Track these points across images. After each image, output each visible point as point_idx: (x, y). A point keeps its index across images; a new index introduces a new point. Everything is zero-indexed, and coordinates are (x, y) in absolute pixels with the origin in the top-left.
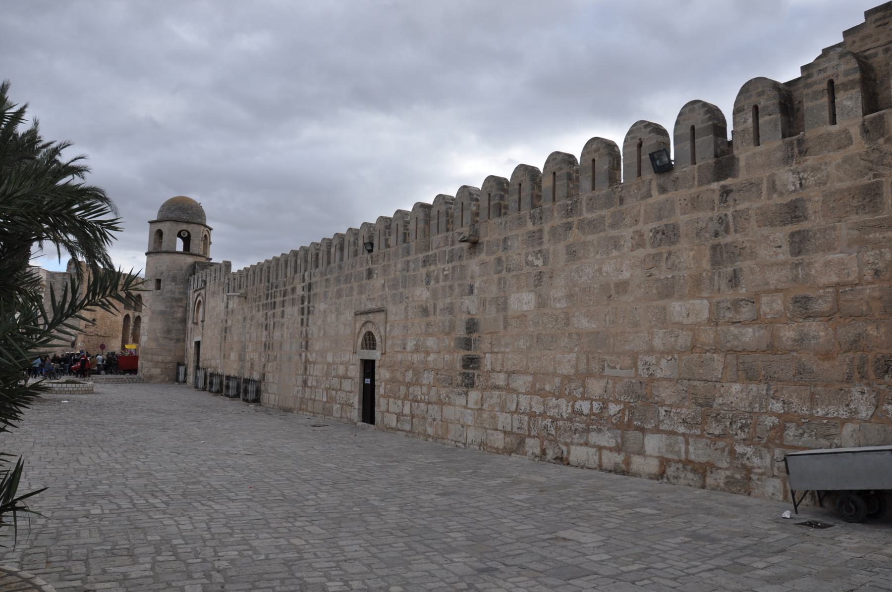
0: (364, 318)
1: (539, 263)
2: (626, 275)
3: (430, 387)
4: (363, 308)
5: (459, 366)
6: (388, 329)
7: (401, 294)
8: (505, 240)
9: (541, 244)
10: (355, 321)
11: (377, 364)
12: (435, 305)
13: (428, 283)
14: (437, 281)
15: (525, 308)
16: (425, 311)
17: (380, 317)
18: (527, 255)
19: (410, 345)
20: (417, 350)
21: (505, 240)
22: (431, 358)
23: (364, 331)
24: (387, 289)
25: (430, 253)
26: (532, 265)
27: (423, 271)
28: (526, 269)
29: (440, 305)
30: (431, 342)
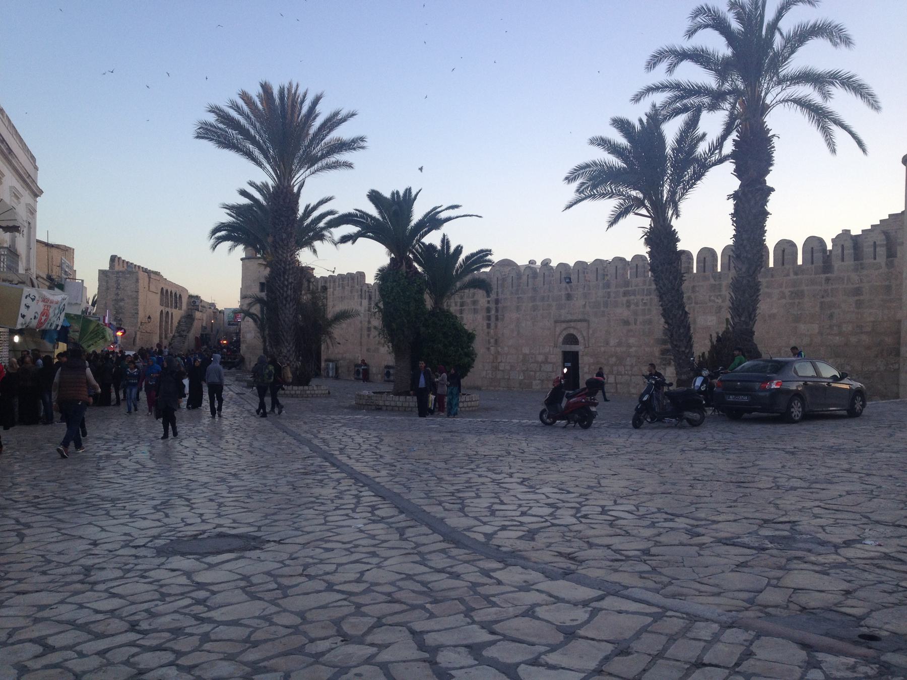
0: (564, 325)
1: (720, 301)
2: (775, 311)
3: (632, 366)
4: (563, 318)
5: (657, 354)
6: (591, 332)
7: (603, 312)
8: (694, 287)
9: (720, 291)
10: (555, 327)
11: (580, 354)
12: (636, 320)
13: (628, 306)
14: (637, 305)
15: (709, 324)
16: (626, 323)
17: (585, 324)
18: (710, 296)
19: (613, 342)
20: (620, 344)
21: (694, 287)
22: (633, 350)
23: (565, 333)
24: (588, 308)
25: (630, 288)
26: (714, 301)
27: (625, 299)
28: (710, 304)
29: (640, 319)
30: (632, 341)
